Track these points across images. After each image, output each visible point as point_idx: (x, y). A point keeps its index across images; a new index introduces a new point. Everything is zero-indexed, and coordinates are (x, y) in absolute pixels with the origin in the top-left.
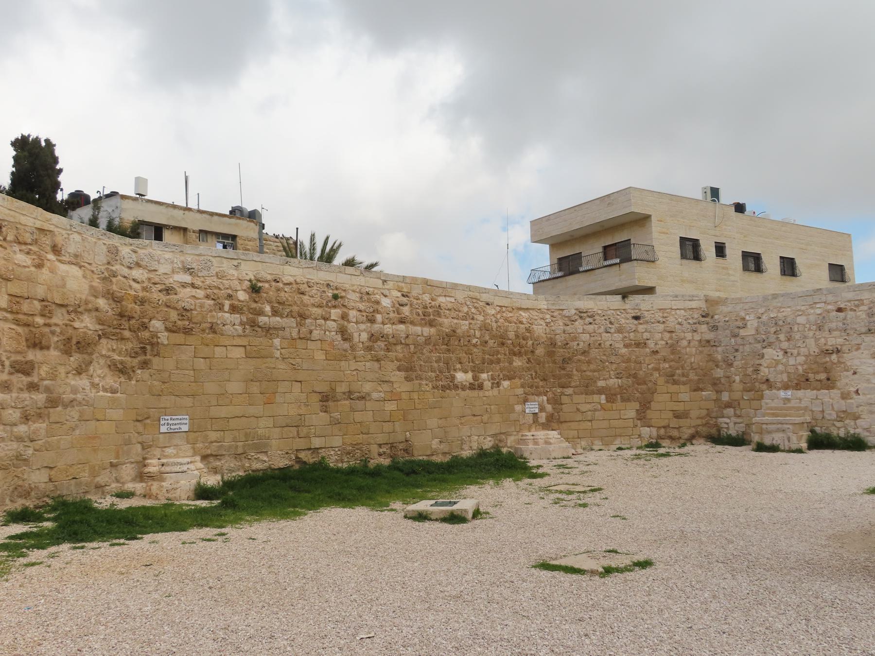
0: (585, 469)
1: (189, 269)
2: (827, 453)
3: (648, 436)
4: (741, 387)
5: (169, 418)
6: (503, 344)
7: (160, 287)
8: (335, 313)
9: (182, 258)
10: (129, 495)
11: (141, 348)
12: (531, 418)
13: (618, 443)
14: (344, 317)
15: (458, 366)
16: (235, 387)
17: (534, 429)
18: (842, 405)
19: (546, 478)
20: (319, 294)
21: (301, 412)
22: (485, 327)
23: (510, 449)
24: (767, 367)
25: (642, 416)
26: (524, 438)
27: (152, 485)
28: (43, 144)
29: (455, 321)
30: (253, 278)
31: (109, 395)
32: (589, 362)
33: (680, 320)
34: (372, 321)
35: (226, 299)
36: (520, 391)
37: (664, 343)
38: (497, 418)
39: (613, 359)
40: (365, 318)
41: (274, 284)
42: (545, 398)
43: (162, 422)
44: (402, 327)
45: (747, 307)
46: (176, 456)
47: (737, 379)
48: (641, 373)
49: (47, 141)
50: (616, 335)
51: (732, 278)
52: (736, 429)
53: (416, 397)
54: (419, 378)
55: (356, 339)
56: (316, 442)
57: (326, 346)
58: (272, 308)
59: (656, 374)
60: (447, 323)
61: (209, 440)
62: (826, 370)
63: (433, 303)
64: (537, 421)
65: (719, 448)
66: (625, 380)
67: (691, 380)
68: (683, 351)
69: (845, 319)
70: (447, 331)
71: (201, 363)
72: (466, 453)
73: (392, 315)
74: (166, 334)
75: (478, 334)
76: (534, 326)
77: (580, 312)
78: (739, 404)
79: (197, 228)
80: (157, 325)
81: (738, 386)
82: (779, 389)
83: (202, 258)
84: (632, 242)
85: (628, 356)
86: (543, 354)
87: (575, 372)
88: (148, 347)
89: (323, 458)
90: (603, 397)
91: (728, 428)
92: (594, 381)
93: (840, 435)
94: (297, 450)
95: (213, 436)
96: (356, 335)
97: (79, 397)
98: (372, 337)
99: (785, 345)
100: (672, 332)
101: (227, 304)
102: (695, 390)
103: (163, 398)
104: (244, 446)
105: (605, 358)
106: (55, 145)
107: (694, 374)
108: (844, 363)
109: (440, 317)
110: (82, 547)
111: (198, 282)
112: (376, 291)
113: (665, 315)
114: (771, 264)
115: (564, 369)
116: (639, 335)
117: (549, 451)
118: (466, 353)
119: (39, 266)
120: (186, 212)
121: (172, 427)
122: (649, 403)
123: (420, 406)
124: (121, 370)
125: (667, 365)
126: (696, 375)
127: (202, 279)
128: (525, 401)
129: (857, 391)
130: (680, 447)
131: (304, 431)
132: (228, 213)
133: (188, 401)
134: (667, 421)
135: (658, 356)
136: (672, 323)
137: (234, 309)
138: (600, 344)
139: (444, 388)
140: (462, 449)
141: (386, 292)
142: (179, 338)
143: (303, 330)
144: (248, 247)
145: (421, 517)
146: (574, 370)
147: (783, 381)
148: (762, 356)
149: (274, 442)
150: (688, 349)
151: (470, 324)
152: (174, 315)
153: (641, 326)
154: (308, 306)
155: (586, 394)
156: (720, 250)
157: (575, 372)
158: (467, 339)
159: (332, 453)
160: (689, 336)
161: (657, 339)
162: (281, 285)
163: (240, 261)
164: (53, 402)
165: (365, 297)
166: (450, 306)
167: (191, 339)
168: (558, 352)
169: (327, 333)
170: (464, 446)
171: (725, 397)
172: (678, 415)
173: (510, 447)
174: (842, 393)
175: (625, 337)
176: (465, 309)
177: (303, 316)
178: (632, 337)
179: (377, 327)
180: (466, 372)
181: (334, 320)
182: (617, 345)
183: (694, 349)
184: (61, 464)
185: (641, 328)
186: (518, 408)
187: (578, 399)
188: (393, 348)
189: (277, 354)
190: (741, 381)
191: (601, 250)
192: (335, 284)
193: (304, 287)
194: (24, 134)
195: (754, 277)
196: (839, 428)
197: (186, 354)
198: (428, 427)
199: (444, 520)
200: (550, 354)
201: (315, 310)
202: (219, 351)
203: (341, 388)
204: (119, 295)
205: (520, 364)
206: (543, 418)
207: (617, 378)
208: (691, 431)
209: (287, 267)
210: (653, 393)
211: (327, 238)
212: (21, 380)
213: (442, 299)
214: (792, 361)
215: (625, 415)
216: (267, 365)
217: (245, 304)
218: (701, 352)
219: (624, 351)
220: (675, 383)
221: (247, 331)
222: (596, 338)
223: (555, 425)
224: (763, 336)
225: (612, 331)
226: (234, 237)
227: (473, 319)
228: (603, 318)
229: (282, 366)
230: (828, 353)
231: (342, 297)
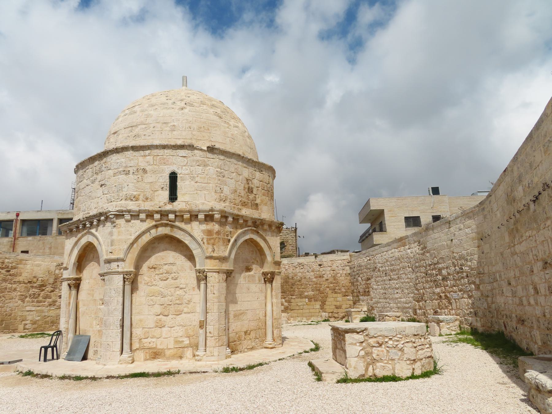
25: (322, 307)
32: (301, 285)
37: (331, 275)
39: (310, 283)
48: (321, 289)
50: (311, 273)
59: (328, 289)
66: (315, 292)
67: (342, 292)
90: (307, 299)
102: (344, 296)
105: (307, 283)
116: (321, 273)
125: (332, 285)
134: (332, 310)
135: (329, 281)
136: (334, 267)
150: (341, 278)
153: (321, 269)
157: (296, 289)
161: (328, 274)
172: (337, 307)
175: (315, 274)
178: (318, 274)
183: (343, 278)
187: (297, 300)
210: (326, 298)
215: (315, 307)
218: (346, 279)
219: (314, 280)
220: (336, 293)
222: (304, 275)
225: (310, 271)
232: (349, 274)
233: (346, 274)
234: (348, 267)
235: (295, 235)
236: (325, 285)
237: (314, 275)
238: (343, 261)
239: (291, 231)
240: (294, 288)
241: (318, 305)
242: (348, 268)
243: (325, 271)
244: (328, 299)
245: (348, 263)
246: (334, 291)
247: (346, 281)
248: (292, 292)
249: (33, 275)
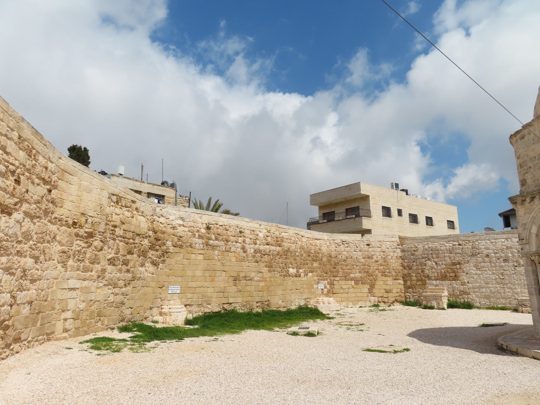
0: (351, 315)
1: (182, 218)
3: (373, 301)
5: (172, 286)
6: (309, 256)
7: (171, 226)
8: (240, 240)
9: (179, 213)
10: (157, 322)
11: (162, 254)
12: (321, 291)
13: (360, 304)
14: (244, 241)
15: (290, 266)
16: (199, 273)
17: (322, 297)
18: (462, 288)
19: (335, 319)
20: (234, 231)
21: (225, 286)
22: (302, 248)
23: (311, 306)
24: (428, 270)
25: (370, 291)
26: (318, 301)
27: (166, 318)
28: (83, 149)
29: (290, 244)
30: (207, 223)
31: (151, 275)
32: (347, 265)
33: (388, 247)
34: (255, 244)
35: (197, 232)
36: (316, 278)
37: (381, 257)
38: (306, 291)
39: (358, 264)
40: (252, 242)
41: (215, 225)
42: (327, 282)
43: (169, 289)
44: (267, 246)
46: (174, 304)
47: (414, 275)
48: (370, 271)
49: (85, 148)
50: (359, 253)
51: (405, 226)
53: (273, 280)
54: (274, 271)
55: (248, 252)
56: (231, 300)
57: (236, 255)
58: (215, 236)
59: (377, 272)
60: (286, 245)
61: (188, 298)
62: (454, 272)
63: (280, 236)
64: (323, 293)
65: (407, 307)
66: (363, 274)
70: (286, 249)
71: (186, 262)
72: (293, 307)
73: (264, 241)
74: (172, 247)
75: (299, 250)
76: (322, 248)
77: (343, 241)
78: (415, 287)
79: (146, 192)
80: (169, 243)
81: (414, 278)
82: (433, 280)
83: (187, 213)
84: (360, 208)
85: (365, 263)
86: (326, 260)
87: (340, 270)
88: (165, 253)
89: (235, 308)
90: (353, 282)
91: (410, 298)
92: (349, 274)
93: (461, 302)
94: (223, 304)
95: (189, 296)
96: (249, 250)
97: (142, 276)
98: (256, 251)
99: (436, 260)
100: (384, 252)
101: (197, 234)
102: (395, 280)
103: (170, 277)
104: (202, 301)
105: (354, 263)
106: (88, 151)
107: (394, 272)
108: (462, 269)
109: (283, 242)
110: (165, 342)
111: (185, 224)
112: (257, 230)
113: (381, 244)
114: (422, 220)
115: (335, 268)
116: (369, 253)
117: (330, 307)
118: (294, 260)
119: (132, 217)
120: (142, 183)
121: (173, 291)
122: (374, 285)
123: (274, 284)
124: (154, 264)
125: (382, 268)
126: (395, 273)
127: (187, 223)
128: (318, 283)
129: (468, 281)
130: (388, 307)
131: (226, 295)
132: (160, 184)
133: (180, 279)
134: (382, 294)
135: (378, 263)
136: (384, 248)
137: (200, 237)
138: (352, 257)
139: (285, 276)
140: (291, 305)
141: (261, 230)
142: (177, 250)
143: (227, 247)
144: (170, 202)
145: (295, 334)
146: (340, 269)
147: (435, 276)
148: (425, 265)
149: (214, 299)
150: (391, 260)
151: (296, 246)
152: (176, 239)
153: (370, 249)
154: (229, 236)
155: (345, 280)
156: (400, 212)
157: (340, 270)
158: (294, 253)
159: (238, 305)
161: (378, 255)
162: (218, 226)
163: (202, 215)
164: (134, 279)
165: (253, 232)
166: (287, 237)
167: (182, 250)
168: (333, 260)
169: (237, 249)
170: (292, 304)
171: (409, 283)
172: (387, 292)
173: (312, 305)
174: (461, 283)
175: (363, 254)
176: (293, 239)
177: (227, 241)
178: (366, 254)
179: (257, 246)
180: (293, 269)
181: (240, 243)
182: (359, 258)
183: (394, 260)
184: (135, 307)
185: (370, 250)
186: (315, 286)
187: (341, 282)
188: (264, 257)
189: (216, 258)
190: (416, 276)
191: (345, 211)
192: (240, 226)
193: (228, 227)
194: (74, 145)
195: (414, 225)
196: (460, 299)
197: (179, 257)
198: (277, 294)
199: (305, 335)
200: (329, 261)
201: (232, 238)
202: (193, 256)
203: (242, 275)
204: (157, 229)
205: (316, 265)
206: (325, 291)
207: (360, 273)
208: (393, 299)
209: (221, 218)
210: (376, 281)
211: (210, 199)
212: (124, 268)
213: (283, 234)
214: (439, 268)
215: (363, 291)
216: (211, 263)
217: (204, 234)
218: (397, 262)
219: (363, 260)
220: (386, 276)
221: (205, 247)
222: (350, 254)
223: (331, 295)
224: (426, 256)
225: (357, 251)
226: (163, 196)
227: (297, 244)
228: (353, 245)
229: (218, 263)
230: (454, 264)
231: (243, 232)
232: (401, 257)
233: (397, 257)
234: (399, 249)
235: (188, 205)
236: (374, 266)
237: (362, 255)
238: (392, 243)
239: (184, 200)
240: (337, 268)
241: (365, 289)
242: (399, 250)
243: (374, 251)
244: (378, 283)
245: (398, 245)
246: (384, 274)
248: (335, 273)
249: (81, 210)
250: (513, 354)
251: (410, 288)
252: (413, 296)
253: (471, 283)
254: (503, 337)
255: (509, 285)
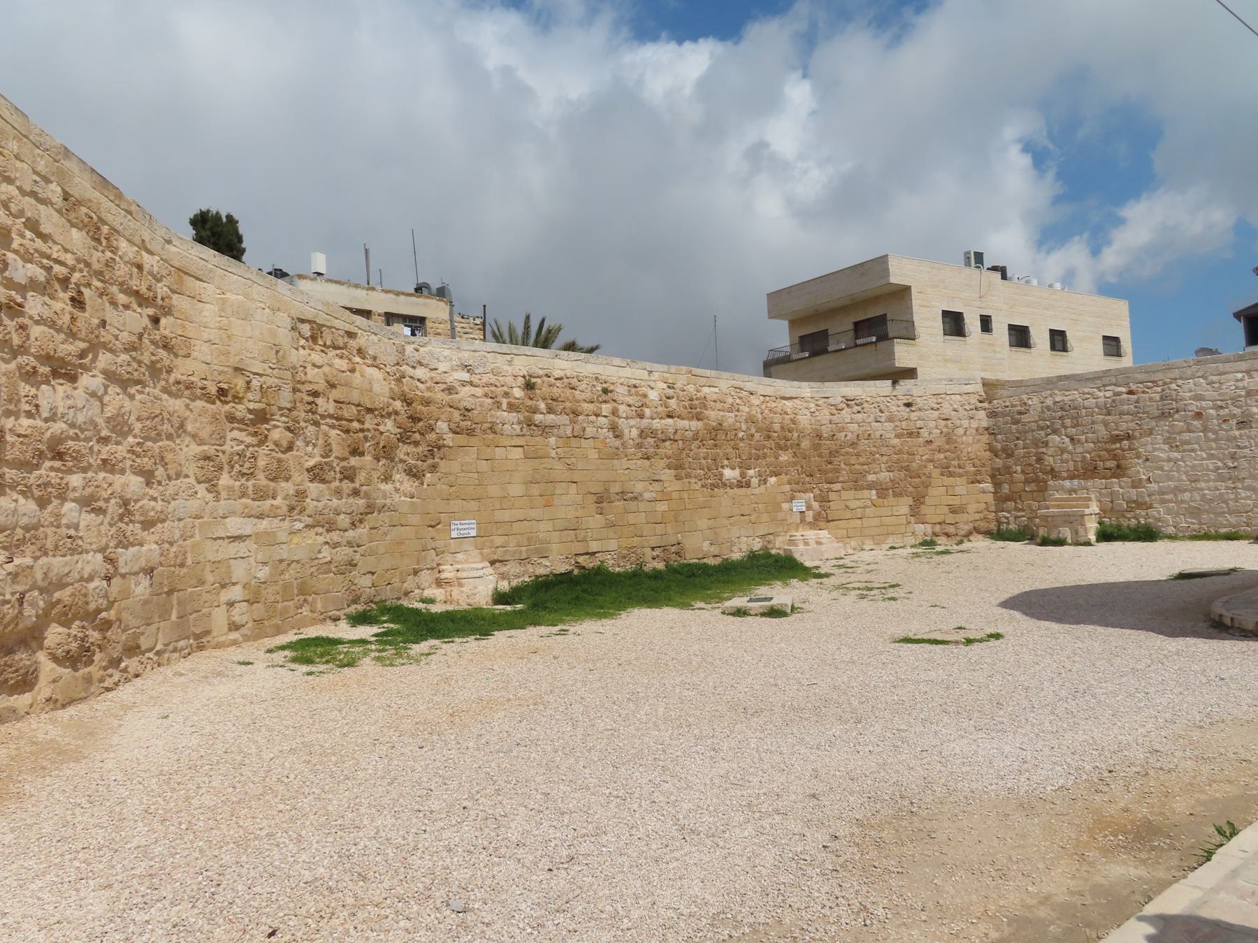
0: (869, 568)
1: (466, 366)
2: (1117, 545)
3: (922, 534)
4: (1022, 477)
5: (458, 522)
6: (769, 437)
7: (443, 386)
8: (606, 409)
9: (460, 355)
10: (432, 601)
11: (429, 451)
12: (799, 517)
13: (891, 541)
14: (615, 412)
15: (726, 462)
16: (516, 490)
17: (801, 529)
19: (833, 577)
20: (589, 389)
21: (578, 514)
22: (751, 420)
23: (778, 551)
26: (793, 538)
27: (452, 591)
28: (224, 220)
29: (721, 413)
30: (526, 373)
31: (409, 499)
32: (858, 455)
33: (956, 406)
34: (641, 416)
35: (503, 397)
36: (787, 488)
37: (939, 431)
38: (765, 517)
39: (884, 450)
40: (634, 413)
41: (545, 379)
42: (812, 495)
43: (453, 527)
44: (670, 420)
45: (1028, 390)
46: (466, 561)
47: (1019, 468)
49: (229, 217)
50: (886, 424)
51: (999, 356)
52: (1018, 523)
53: (686, 496)
54: (688, 476)
55: (626, 437)
56: (594, 546)
57: (600, 445)
58: (547, 404)
59: (931, 466)
60: (713, 415)
61: (496, 545)
62: (1115, 457)
63: (699, 394)
64: (805, 520)
66: (896, 474)
68: (959, 440)
69: (1137, 402)
70: (714, 424)
71: (483, 466)
72: (736, 556)
73: (660, 409)
74: (451, 435)
75: (744, 427)
76: (798, 417)
77: (847, 400)
78: (1020, 496)
79: (382, 311)
80: (442, 426)
81: (1019, 477)
83: (478, 353)
84: (889, 317)
85: (900, 447)
86: (808, 446)
87: (843, 466)
88: (435, 450)
89: (602, 562)
90: (874, 492)
91: (1008, 523)
92: (863, 474)
93: (1131, 526)
94: (576, 555)
95: (499, 540)
96: (626, 431)
97: (388, 501)
98: (642, 434)
100: (947, 419)
101: (505, 402)
102: (972, 482)
103: (452, 502)
104: (527, 551)
105: (875, 449)
106: (237, 222)
108: (1135, 449)
109: (706, 410)
110: (452, 642)
111: (475, 379)
112: (643, 383)
113: (940, 400)
114: (1040, 338)
115: (830, 463)
116: (912, 424)
117: (822, 551)
118: (733, 449)
119: (352, 371)
120: (370, 292)
121: (461, 532)
122: (923, 497)
123: (690, 506)
124: (413, 474)
125: (942, 456)
126: (974, 466)
127: (479, 376)
128: (792, 499)
129: (1149, 478)
130: (957, 545)
131: (581, 534)
132: (413, 292)
133: (474, 505)
134: (942, 517)
135: (934, 446)
136: (947, 410)
137: (512, 407)
138: (869, 435)
139: (713, 486)
140: (732, 551)
141: (652, 384)
142: (462, 439)
143: (577, 427)
144: (439, 331)
145: (740, 613)
146: (842, 464)
147: (1068, 470)
148: (1046, 444)
149: (554, 547)
150: (964, 438)
151: (736, 416)
152: (456, 415)
154: (579, 402)
155: (856, 489)
156: (986, 323)
157: (843, 466)
158: (734, 432)
159: (609, 557)
160: (965, 423)
161: (931, 428)
162: (552, 380)
163: (512, 356)
164: (370, 509)
165: (633, 390)
166: (715, 396)
167: (473, 441)
168: (825, 444)
169: (599, 430)
170: (734, 548)
171: (1006, 489)
172: (954, 510)
173: (779, 549)
174: (1133, 481)
175: (897, 426)
176: (730, 400)
177: (576, 413)
178: (904, 427)
179: (645, 422)
180: (733, 468)
181: (605, 416)
182: (888, 436)
184: (379, 571)
185: (914, 416)
186: (785, 506)
187: (845, 495)
188: (662, 445)
189: (553, 454)
190: (1023, 472)
191: (852, 327)
192: (604, 377)
193: (574, 382)
194: (203, 210)
195: (1021, 353)
196: (1129, 519)
197: (470, 456)
198: (699, 528)
199: (763, 615)
200: (816, 447)
201: (585, 405)
202: (499, 452)
203: (616, 488)
204: (411, 396)
205: (786, 458)
206: (810, 516)
207: (889, 471)
208: (967, 528)
209: (557, 360)
210: (928, 487)
211: (528, 318)
212: (347, 486)
213: (706, 390)
214: (1079, 450)
215: (897, 511)
216: (543, 466)
217: (521, 401)
218: (979, 441)
219: (896, 441)
220: (951, 475)
221: (524, 430)
222: (864, 428)
223: (822, 524)
225: (883, 420)
226: (422, 320)
227: (738, 411)
228: (872, 406)
229: (558, 466)
230: (1116, 439)
231: (611, 392)
232: (987, 429)
234: (983, 412)
235: (482, 337)
236: (923, 453)
237: (894, 430)
238: (966, 397)
239: (472, 326)
240: (836, 463)
241: (903, 506)
242: (982, 414)
243: (924, 420)
244: (933, 492)
245: (981, 402)
246: (946, 471)
247: (977, 447)
249: (234, 361)
250: (1245, 636)
251: (1009, 500)
252: (1016, 518)
253: (1155, 482)
254: (1225, 599)
255: (1248, 482)
